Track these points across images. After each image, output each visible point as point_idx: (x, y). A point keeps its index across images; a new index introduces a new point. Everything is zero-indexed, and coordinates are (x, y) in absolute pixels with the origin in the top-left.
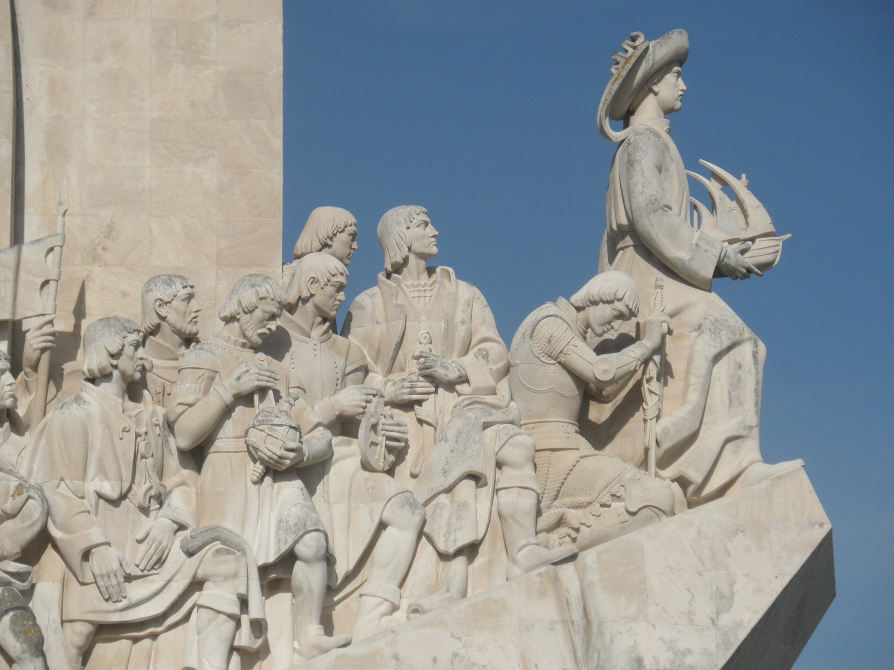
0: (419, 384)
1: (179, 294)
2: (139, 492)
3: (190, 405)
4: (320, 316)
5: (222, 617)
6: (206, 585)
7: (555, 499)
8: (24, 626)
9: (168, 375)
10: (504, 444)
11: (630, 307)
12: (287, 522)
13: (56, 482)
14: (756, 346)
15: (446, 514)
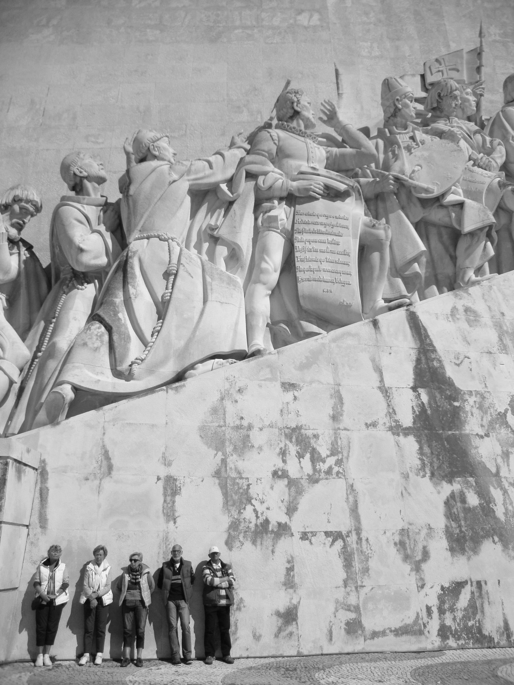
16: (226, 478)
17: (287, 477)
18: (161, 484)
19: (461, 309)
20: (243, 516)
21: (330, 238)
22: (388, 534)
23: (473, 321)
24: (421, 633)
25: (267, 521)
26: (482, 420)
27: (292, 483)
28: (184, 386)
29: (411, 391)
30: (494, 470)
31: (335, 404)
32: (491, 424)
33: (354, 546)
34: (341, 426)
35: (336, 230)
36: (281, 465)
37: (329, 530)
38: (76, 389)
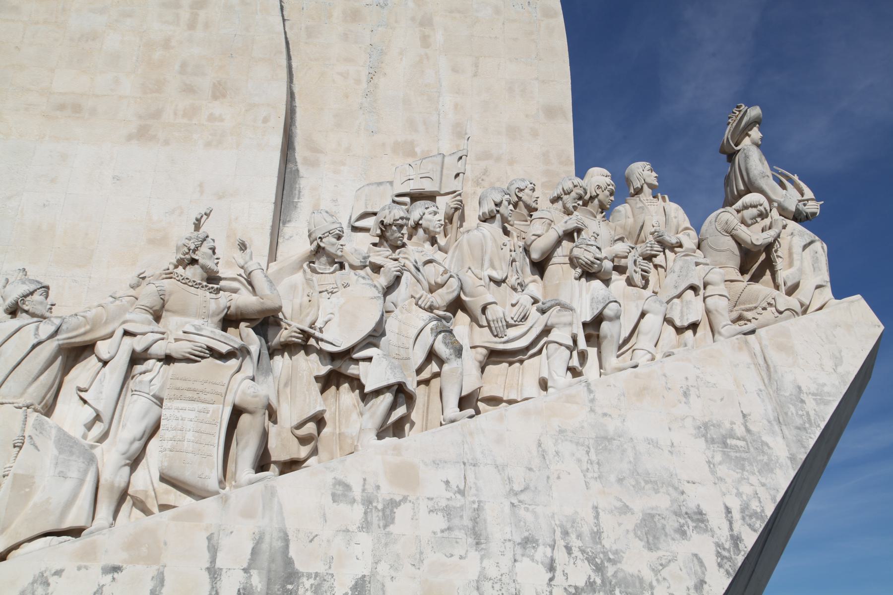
0: (656, 246)
1: (528, 186)
2: (512, 280)
3: (539, 236)
4: (600, 208)
5: (563, 348)
6: (552, 331)
7: (735, 306)
8: (451, 339)
9: (522, 228)
10: (708, 273)
11: (767, 209)
12: (597, 298)
13: (467, 269)
14: (822, 244)
15: (679, 308)
21: (202, 406)
23: (339, 495)
29: (242, 573)
35: (209, 397)
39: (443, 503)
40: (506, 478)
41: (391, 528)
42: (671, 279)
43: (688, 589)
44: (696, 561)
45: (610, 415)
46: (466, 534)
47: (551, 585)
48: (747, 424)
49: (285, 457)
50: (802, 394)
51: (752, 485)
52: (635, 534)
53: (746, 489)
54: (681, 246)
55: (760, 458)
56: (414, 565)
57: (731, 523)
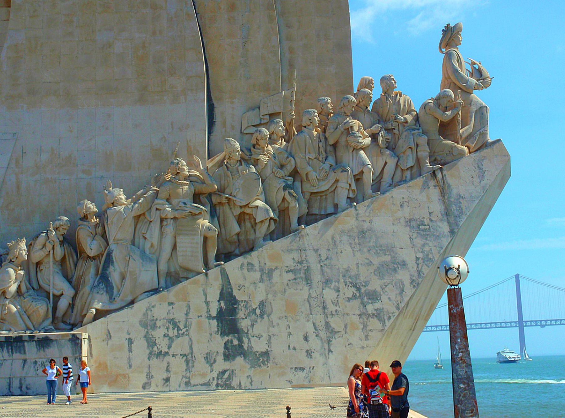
16: (148, 338)
17: (169, 336)
18: (127, 341)
19: (246, 264)
20: (153, 350)
22: (202, 354)
24: (210, 385)
25: (161, 351)
26: (245, 312)
27: (170, 338)
28: (133, 306)
29: (217, 302)
30: (246, 331)
31: (187, 309)
32: (249, 313)
33: (190, 358)
34: (189, 317)
36: (167, 332)
37: (182, 353)
38: (97, 310)
39: (292, 268)
40: (318, 255)
41: (272, 281)
42: (400, 142)
43: (396, 294)
44: (400, 283)
45: (365, 221)
46: (302, 280)
47: (338, 298)
48: (431, 217)
49: (226, 251)
50: (460, 199)
51: (430, 246)
52: (374, 274)
53: (427, 249)
54: (407, 122)
55: (434, 234)
56: (282, 294)
57: (418, 264)
